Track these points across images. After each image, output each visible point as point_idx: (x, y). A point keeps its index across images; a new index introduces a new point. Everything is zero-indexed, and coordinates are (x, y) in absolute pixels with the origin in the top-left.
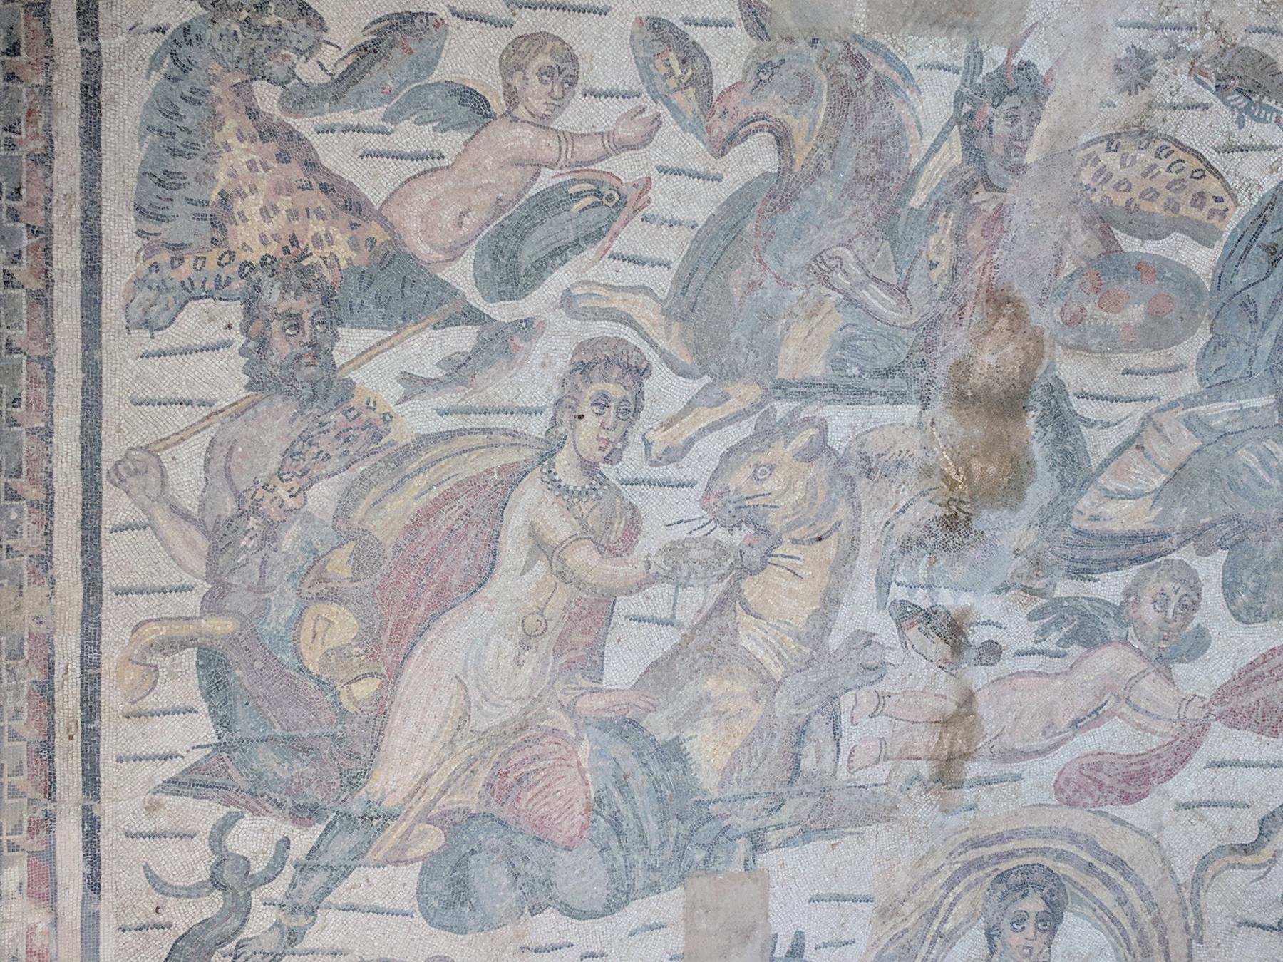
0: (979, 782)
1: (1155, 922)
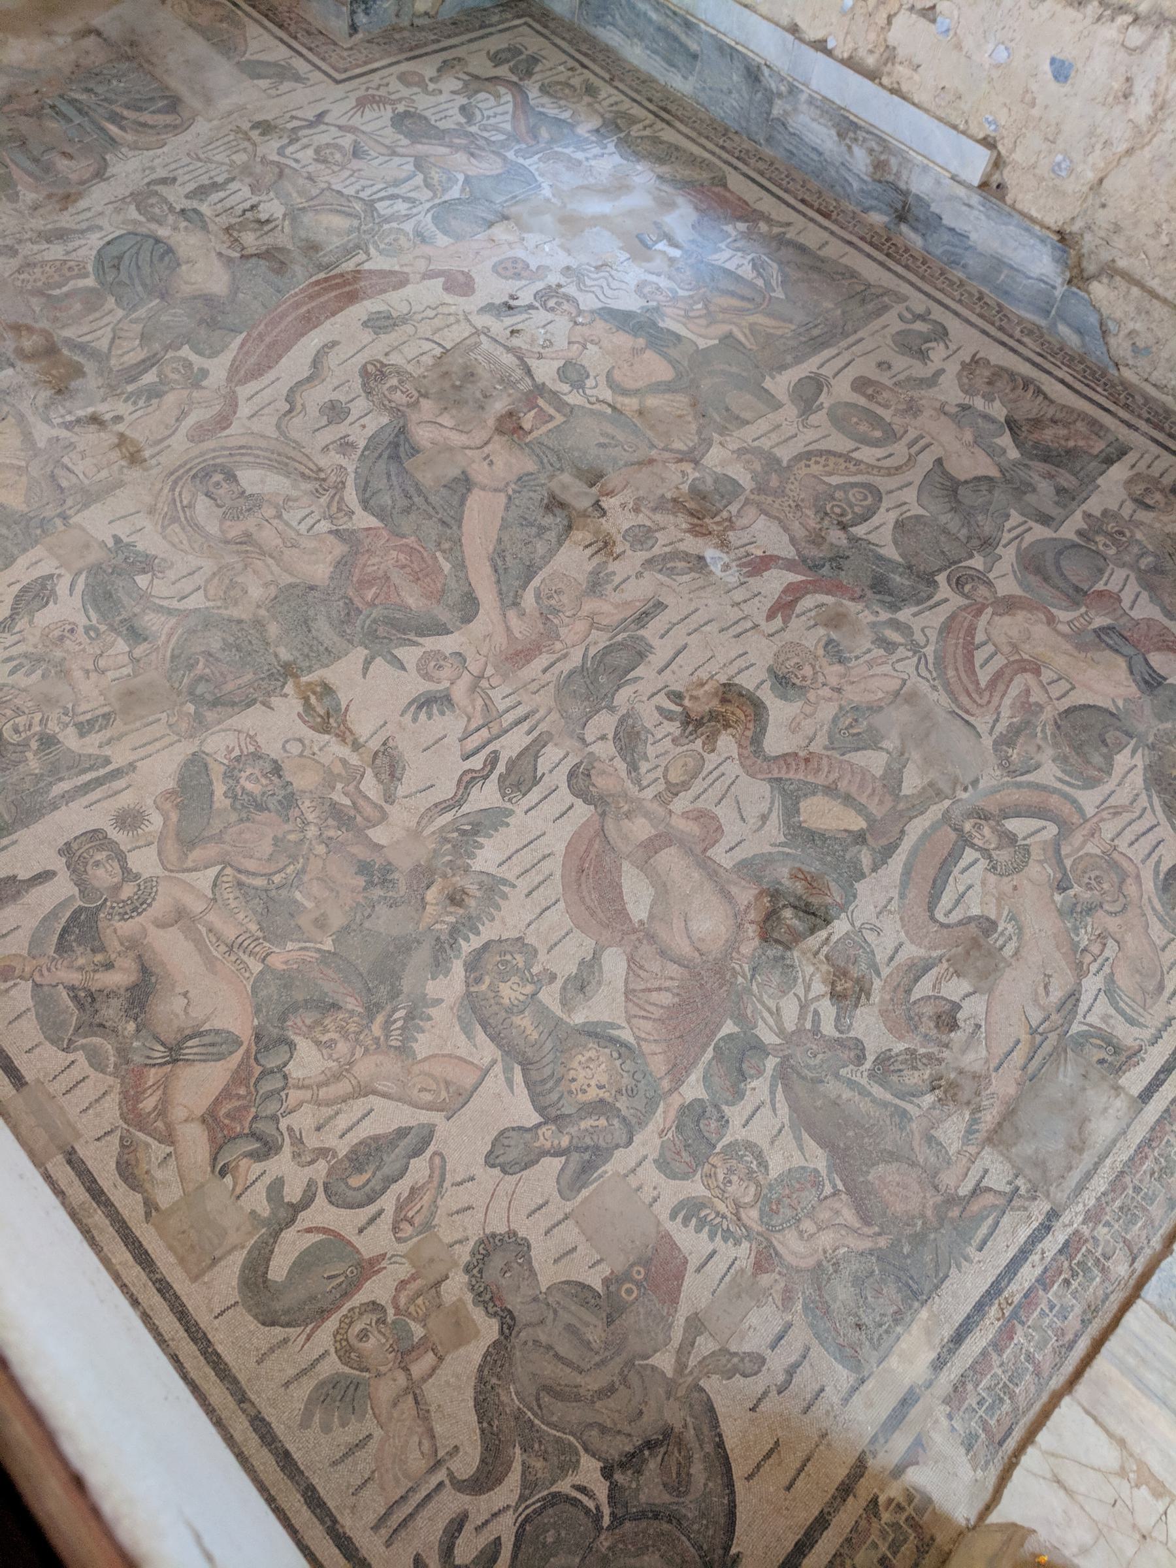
0: (153, 456)
1: (279, 454)
